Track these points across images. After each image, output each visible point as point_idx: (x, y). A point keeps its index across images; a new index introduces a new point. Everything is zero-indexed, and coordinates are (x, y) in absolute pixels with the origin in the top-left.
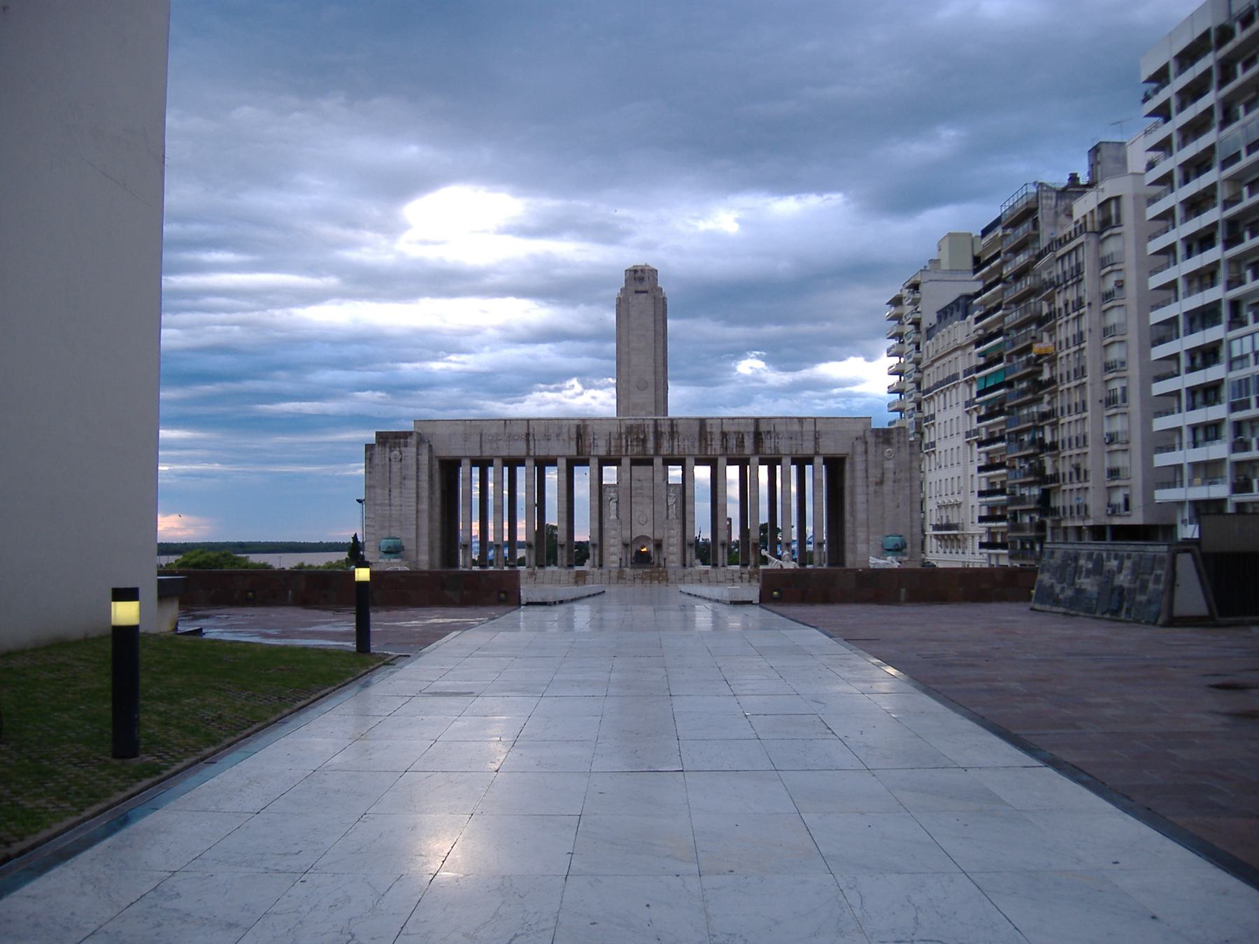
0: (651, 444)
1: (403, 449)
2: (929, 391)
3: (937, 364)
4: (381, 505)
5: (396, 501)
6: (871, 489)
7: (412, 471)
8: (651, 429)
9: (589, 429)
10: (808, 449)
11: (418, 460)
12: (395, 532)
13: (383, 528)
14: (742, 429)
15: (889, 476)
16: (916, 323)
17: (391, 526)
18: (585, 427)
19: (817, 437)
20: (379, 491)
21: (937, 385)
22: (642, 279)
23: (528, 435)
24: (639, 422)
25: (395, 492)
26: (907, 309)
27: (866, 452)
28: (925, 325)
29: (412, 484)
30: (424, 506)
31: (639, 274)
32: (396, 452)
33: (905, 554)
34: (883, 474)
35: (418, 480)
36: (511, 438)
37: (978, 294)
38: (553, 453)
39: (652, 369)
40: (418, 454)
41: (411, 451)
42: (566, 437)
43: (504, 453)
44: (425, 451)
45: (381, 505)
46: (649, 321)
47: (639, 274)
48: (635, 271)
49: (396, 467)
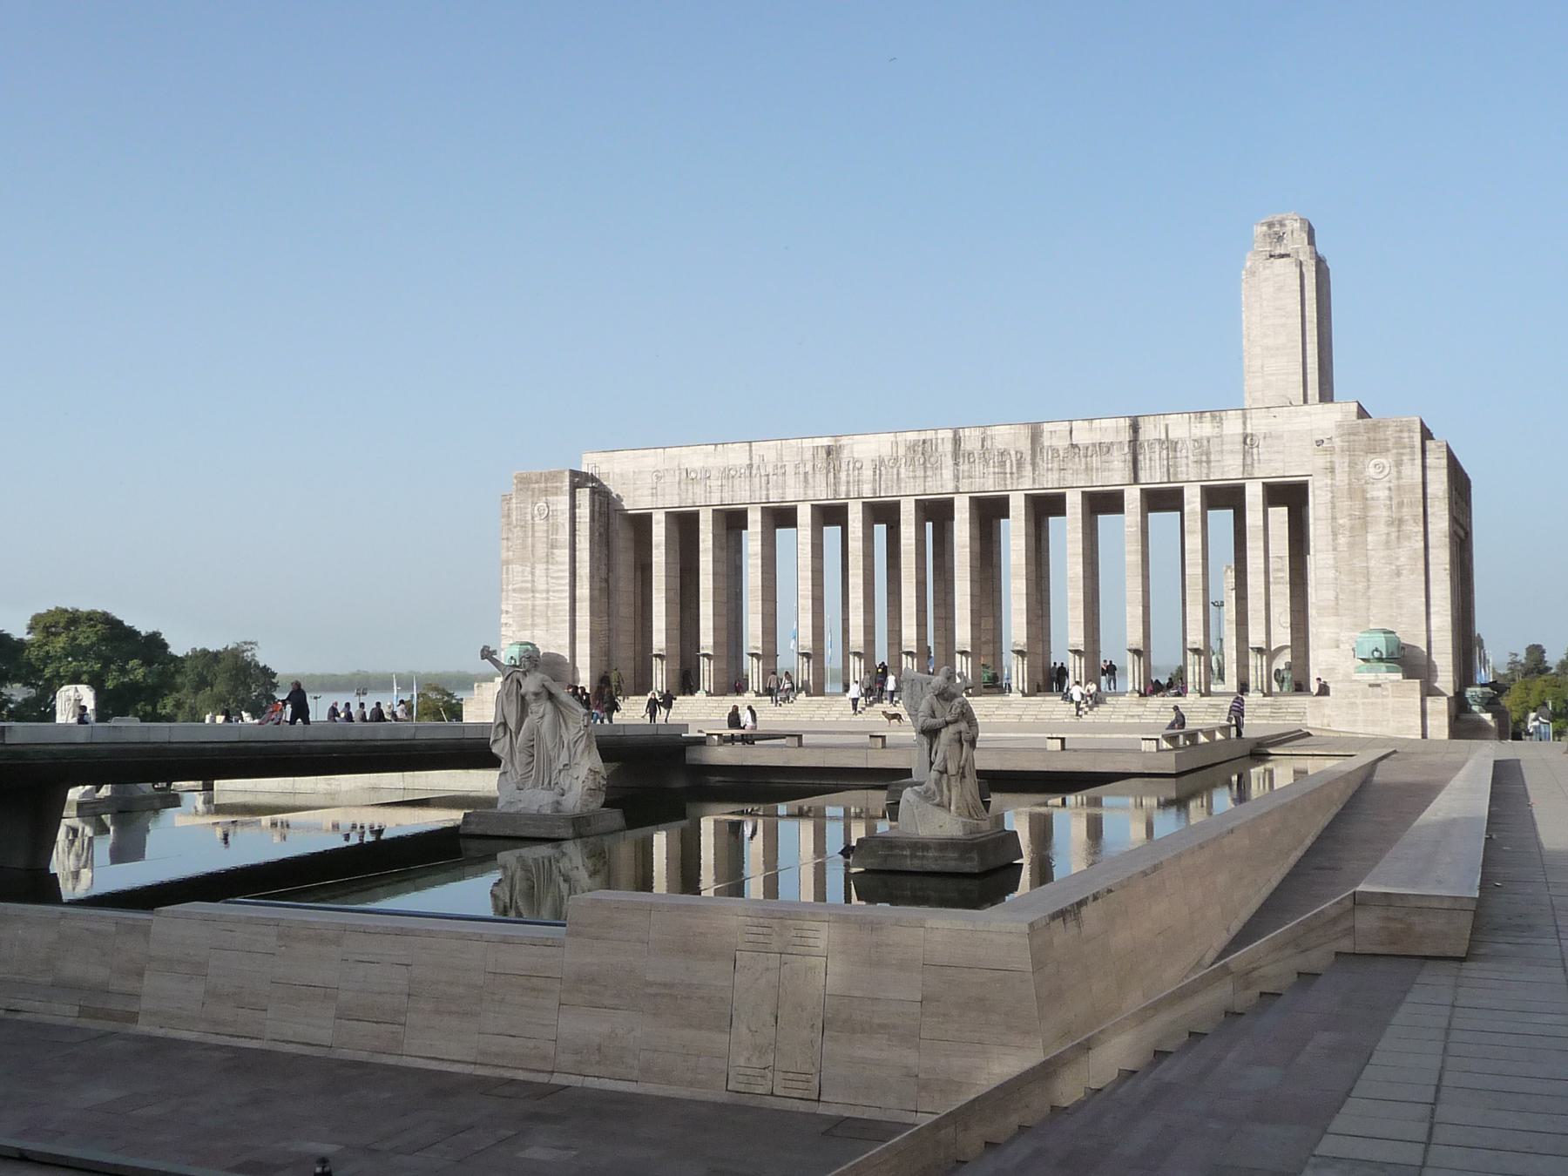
0: (948, 473)
4: (522, 590)
5: (541, 584)
6: (1342, 540)
7: (564, 536)
8: (949, 447)
9: (845, 455)
10: (1227, 470)
13: (523, 627)
15: (1381, 513)
17: (533, 625)
20: (516, 568)
22: (1280, 238)
23: (750, 466)
24: (929, 435)
25: (540, 569)
27: (1332, 470)
29: (563, 554)
31: (1277, 228)
32: (542, 504)
34: (1365, 508)
36: (727, 474)
41: (564, 501)
42: (809, 468)
44: (584, 496)
45: (522, 590)
47: (1277, 228)
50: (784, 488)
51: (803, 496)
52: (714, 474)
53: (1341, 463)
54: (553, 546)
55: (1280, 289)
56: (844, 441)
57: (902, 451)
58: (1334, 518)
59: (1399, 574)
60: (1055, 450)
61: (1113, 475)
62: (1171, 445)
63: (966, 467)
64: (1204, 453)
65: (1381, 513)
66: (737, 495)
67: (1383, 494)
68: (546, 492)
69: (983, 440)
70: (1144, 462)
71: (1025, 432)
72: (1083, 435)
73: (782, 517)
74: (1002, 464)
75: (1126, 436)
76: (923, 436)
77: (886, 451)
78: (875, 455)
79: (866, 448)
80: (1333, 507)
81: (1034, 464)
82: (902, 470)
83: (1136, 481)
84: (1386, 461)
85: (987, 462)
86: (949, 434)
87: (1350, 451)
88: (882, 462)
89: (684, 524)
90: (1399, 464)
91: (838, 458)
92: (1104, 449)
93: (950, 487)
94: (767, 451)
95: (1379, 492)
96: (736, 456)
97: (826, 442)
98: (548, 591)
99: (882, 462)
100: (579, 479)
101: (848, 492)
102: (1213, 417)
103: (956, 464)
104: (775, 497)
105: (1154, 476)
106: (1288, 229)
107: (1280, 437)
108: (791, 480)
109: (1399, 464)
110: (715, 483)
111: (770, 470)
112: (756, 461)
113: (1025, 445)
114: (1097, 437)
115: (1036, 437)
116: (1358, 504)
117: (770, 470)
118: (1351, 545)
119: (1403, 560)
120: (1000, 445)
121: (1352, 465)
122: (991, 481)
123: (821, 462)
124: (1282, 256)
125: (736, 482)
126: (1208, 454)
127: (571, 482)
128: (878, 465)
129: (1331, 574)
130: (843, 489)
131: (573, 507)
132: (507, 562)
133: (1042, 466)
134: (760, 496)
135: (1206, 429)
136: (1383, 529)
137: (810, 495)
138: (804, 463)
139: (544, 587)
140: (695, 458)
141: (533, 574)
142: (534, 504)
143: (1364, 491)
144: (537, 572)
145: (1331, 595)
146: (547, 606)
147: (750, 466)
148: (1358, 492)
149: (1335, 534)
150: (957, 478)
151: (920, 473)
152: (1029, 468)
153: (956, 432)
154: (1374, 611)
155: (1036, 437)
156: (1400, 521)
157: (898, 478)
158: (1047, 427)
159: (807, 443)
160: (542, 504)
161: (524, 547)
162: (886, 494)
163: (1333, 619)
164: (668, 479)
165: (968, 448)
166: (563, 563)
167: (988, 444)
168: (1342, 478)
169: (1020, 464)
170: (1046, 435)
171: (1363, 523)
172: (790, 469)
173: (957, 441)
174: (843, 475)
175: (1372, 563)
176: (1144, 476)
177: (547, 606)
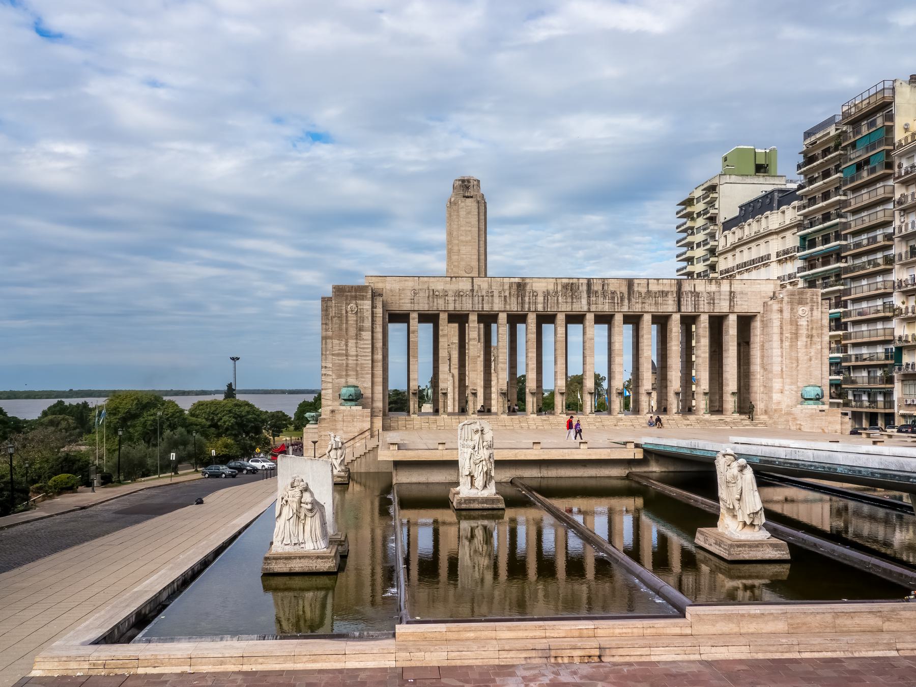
0: (584, 301)
1: (359, 302)
2: (727, 271)
3: (738, 250)
4: (338, 355)
5: (352, 351)
7: (368, 324)
8: (585, 288)
9: (528, 288)
10: (722, 307)
11: (373, 313)
12: (352, 381)
13: (340, 377)
14: (666, 289)
15: (803, 332)
16: (712, 219)
17: (347, 375)
18: (525, 285)
19: (732, 295)
20: (336, 342)
21: (738, 267)
22: (468, 188)
23: (472, 290)
24: (575, 281)
25: (352, 343)
26: (699, 207)
27: (781, 311)
28: (721, 219)
29: (367, 335)
32: (353, 305)
33: (823, 404)
34: (797, 329)
35: (373, 332)
36: (459, 294)
37: (801, 187)
38: (496, 308)
39: (476, 257)
41: (366, 305)
42: (507, 294)
43: (451, 307)
45: (338, 355)
46: (474, 221)
48: (463, 181)
49: (352, 318)
50: (492, 303)
52: (450, 293)
53: (786, 308)
54: (360, 329)
55: (469, 213)
57: (559, 288)
58: (781, 333)
59: (810, 360)
60: (640, 293)
61: (669, 306)
62: (696, 294)
63: (594, 299)
64: (712, 301)
65: (803, 332)
66: (466, 305)
67: (805, 323)
68: (355, 298)
69: (603, 285)
70: (683, 302)
71: (625, 283)
73: (488, 319)
74: (613, 298)
75: (674, 289)
76: (571, 281)
77: (551, 287)
80: (781, 328)
81: (629, 300)
82: (560, 298)
83: (679, 310)
84: (807, 308)
85: (605, 297)
86: (586, 281)
87: (791, 302)
88: (548, 293)
90: (812, 310)
91: (524, 290)
92: (664, 294)
93: (585, 308)
95: (803, 322)
98: (357, 356)
99: (548, 293)
101: (529, 308)
102: (716, 282)
103: (589, 297)
104: (487, 308)
105: (688, 308)
106: (472, 184)
107: (746, 294)
108: (496, 300)
109: (812, 310)
110: (451, 299)
111: (484, 293)
112: (476, 288)
113: (624, 289)
114: (661, 288)
116: (794, 328)
117: (484, 293)
118: (791, 346)
119: (813, 354)
120: (612, 288)
121: (792, 309)
122: (607, 307)
123: (514, 291)
124: (468, 197)
125: (464, 299)
126: (714, 300)
128: (547, 295)
129: (779, 359)
130: (527, 306)
131: (373, 307)
133: (633, 300)
134: (478, 307)
135: (713, 288)
136: (805, 339)
137: (508, 308)
139: (354, 353)
141: (347, 345)
142: (347, 304)
143: (797, 322)
144: (350, 344)
145: (779, 369)
146: (357, 364)
147: (472, 290)
148: (794, 322)
149: (782, 341)
150: (589, 304)
151: (569, 300)
152: (626, 301)
154: (800, 376)
156: (812, 336)
157: (558, 302)
161: (341, 329)
162: (551, 309)
163: (781, 380)
164: (421, 294)
165: (596, 289)
167: (606, 287)
168: (787, 315)
169: (622, 299)
170: (636, 285)
171: (796, 336)
172: (496, 294)
174: (527, 299)
175: (800, 355)
176: (683, 309)
177: (357, 364)
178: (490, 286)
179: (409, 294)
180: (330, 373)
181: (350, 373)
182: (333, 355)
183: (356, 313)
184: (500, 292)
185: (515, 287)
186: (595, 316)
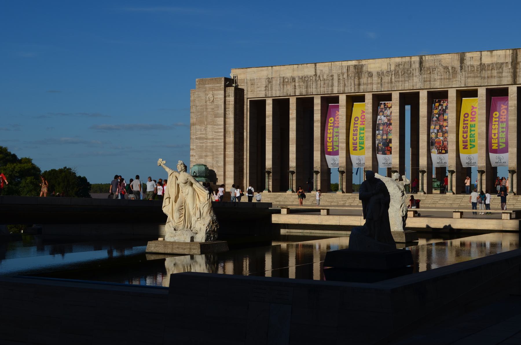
1: (215, 92)
8: (417, 65)
9: (364, 69)
13: (201, 157)
17: (206, 156)
20: (198, 127)
23: (316, 75)
29: (221, 120)
30: (231, 139)
36: (304, 79)
40: (225, 97)
42: (345, 76)
44: (231, 91)
49: (210, 107)
51: (343, 89)
52: (297, 79)
56: (364, 62)
57: (393, 68)
72: (487, 58)
78: (379, 70)
79: (374, 65)
82: (393, 78)
89: (282, 105)
94: (323, 68)
96: (308, 70)
97: (354, 63)
100: (229, 82)
108: (336, 83)
111: (325, 77)
112: (318, 73)
114: (495, 60)
115: (462, 60)
117: (325, 77)
127: (225, 83)
128: (380, 75)
132: (194, 124)
138: (343, 74)
140: (287, 71)
141: (205, 130)
147: (316, 75)
153: (421, 58)
155: (462, 60)
158: (468, 55)
159: (345, 64)
160: (210, 95)
162: (385, 89)
166: (220, 125)
172: (336, 77)
173: (421, 63)
178: (331, 70)
179: (264, 83)
180: (195, 154)
181: (209, 154)
182: (196, 138)
183: (213, 101)
184: (339, 76)
185: (352, 69)
186: (457, 91)
